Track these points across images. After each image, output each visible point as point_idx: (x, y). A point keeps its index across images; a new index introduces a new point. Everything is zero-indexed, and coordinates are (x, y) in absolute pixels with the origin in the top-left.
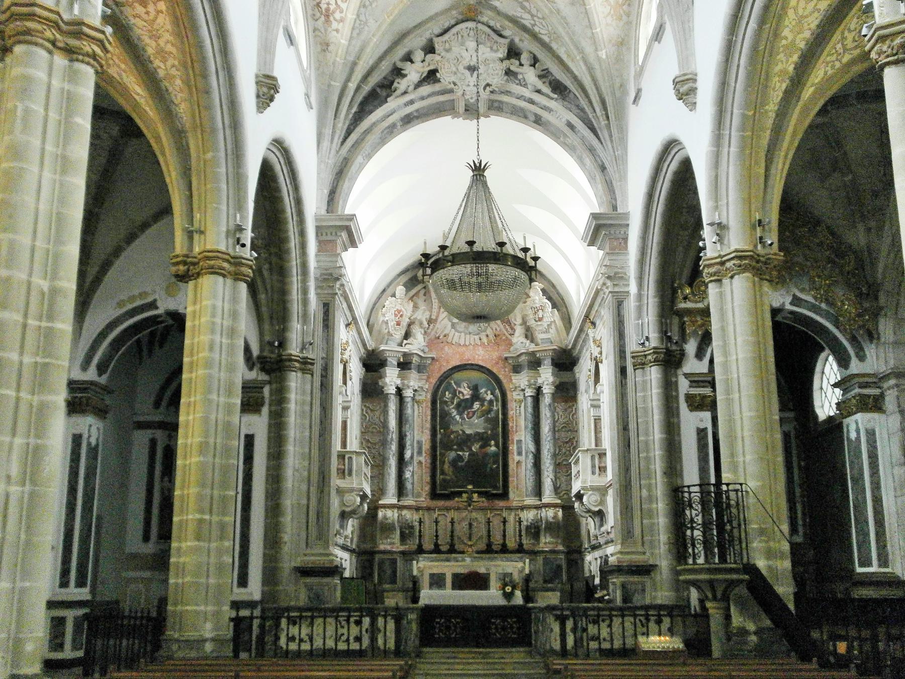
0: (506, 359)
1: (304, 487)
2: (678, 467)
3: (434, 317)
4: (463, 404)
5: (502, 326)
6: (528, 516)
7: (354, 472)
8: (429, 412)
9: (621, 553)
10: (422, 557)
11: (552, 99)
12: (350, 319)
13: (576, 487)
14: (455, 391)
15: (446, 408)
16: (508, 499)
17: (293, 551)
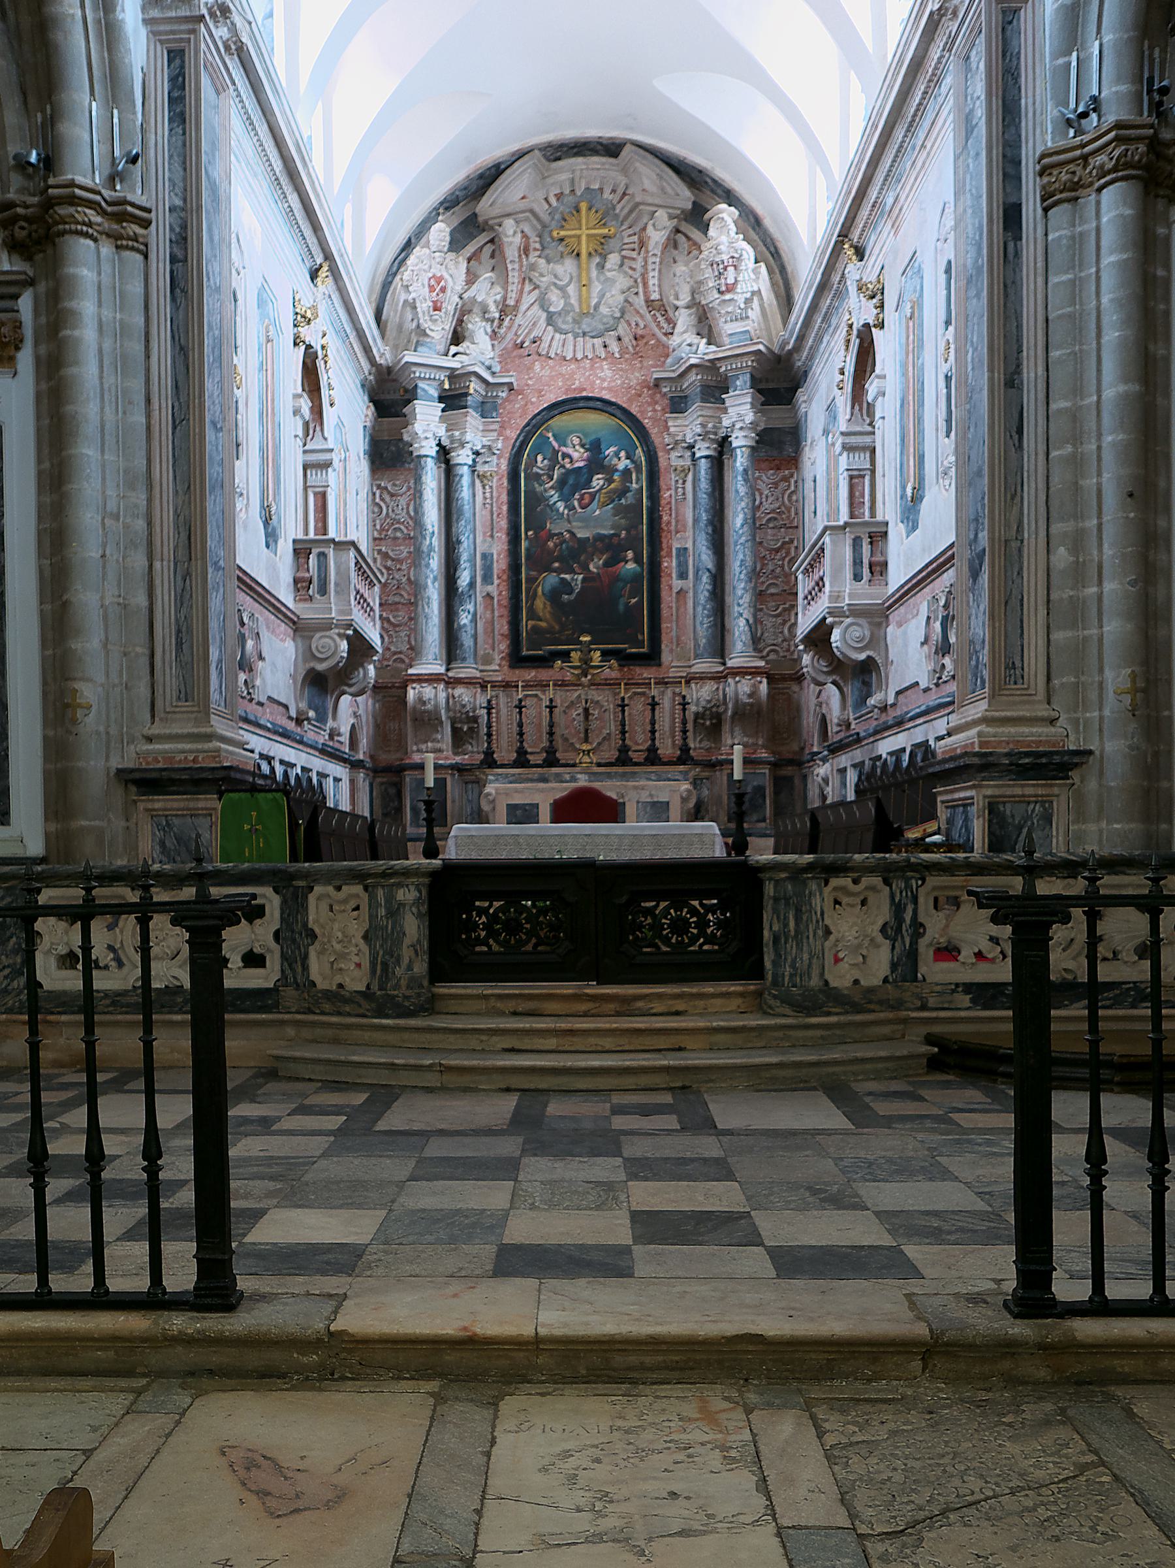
1: (139, 560)
2: (1162, 484)
3: (511, 302)
5: (648, 317)
6: (700, 694)
8: (504, 497)
9: (985, 720)
10: (491, 774)
14: (556, 452)
15: (539, 489)
16: (660, 665)
17: (113, 731)
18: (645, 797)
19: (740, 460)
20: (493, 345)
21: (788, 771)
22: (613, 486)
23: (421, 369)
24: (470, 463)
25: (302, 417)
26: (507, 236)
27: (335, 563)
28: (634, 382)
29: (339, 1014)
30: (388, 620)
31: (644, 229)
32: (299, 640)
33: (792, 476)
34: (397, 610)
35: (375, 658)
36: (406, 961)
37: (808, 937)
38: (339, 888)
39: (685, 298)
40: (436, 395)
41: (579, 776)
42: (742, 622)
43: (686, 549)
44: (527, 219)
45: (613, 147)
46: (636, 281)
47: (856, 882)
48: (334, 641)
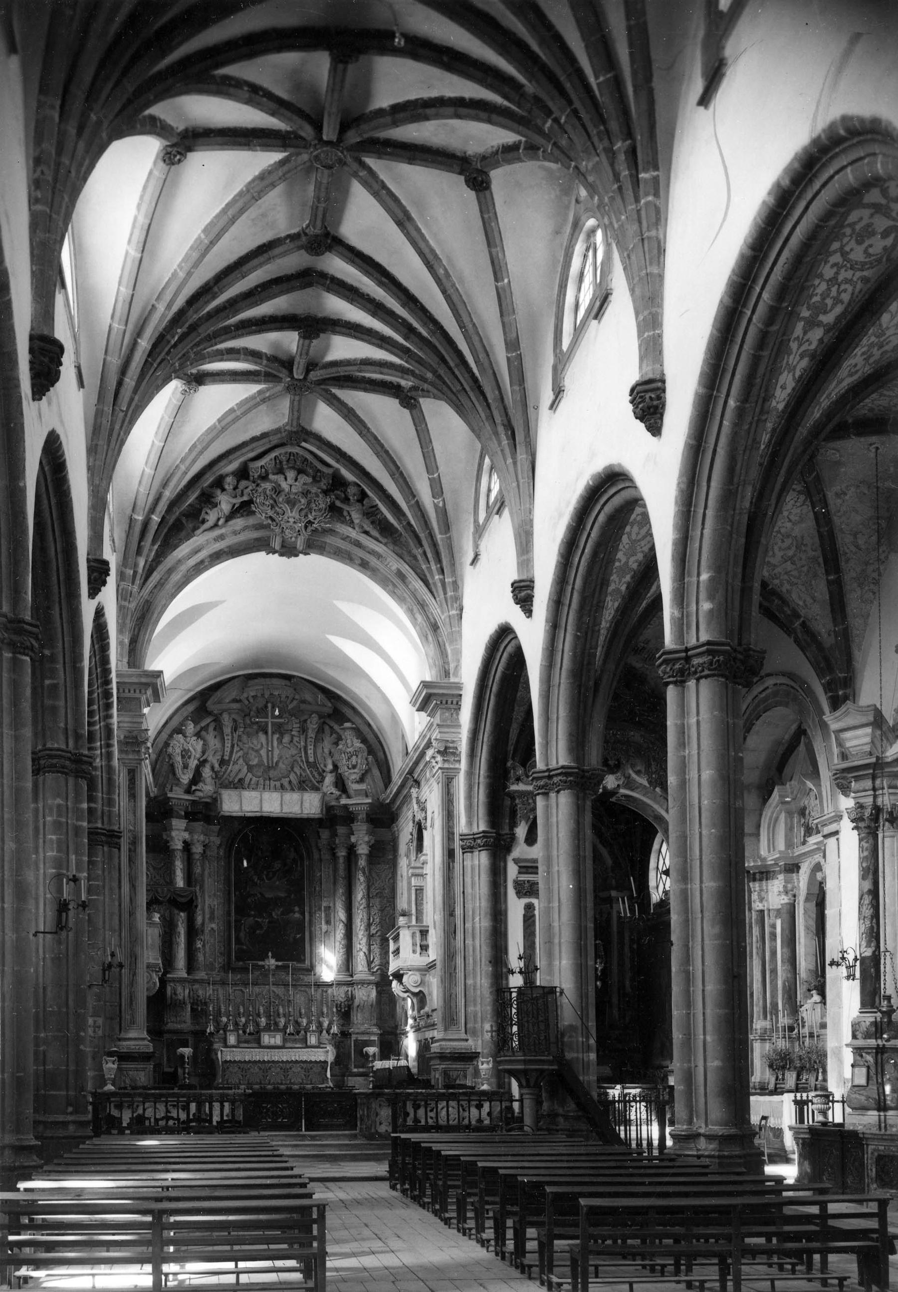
3: (226, 758)
11: (381, 542)
13: (392, 968)
31: (305, 721)
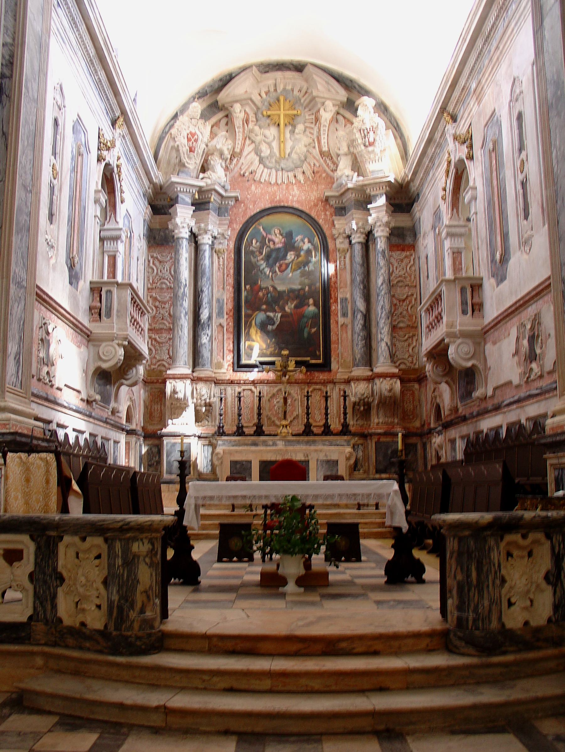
0: (327, 199)
3: (237, 150)
4: (274, 255)
5: (322, 161)
7: (114, 312)
8: (232, 264)
12: (118, 113)
14: (264, 238)
16: (330, 371)
18: (322, 457)
19: (381, 244)
20: (226, 175)
21: (413, 440)
22: (300, 259)
23: (182, 186)
24: (210, 243)
25: (101, 205)
26: (235, 113)
27: (118, 297)
28: (313, 198)
29: (81, 648)
30: (155, 340)
31: (319, 111)
32: (91, 348)
33: (412, 255)
34: (161, 333)
35: (144, 362)
36: (139, 605)
37: (488, 586)
38: (84, 539)
39: (344, 149)
40: (190, 201)
41: (278, 442)
42: (383, 345)
43: (346, 299)
44: (248, 104)
45: (299, 67)
46: (314, 140)
47: (524, 537)
48: (115, 349)
